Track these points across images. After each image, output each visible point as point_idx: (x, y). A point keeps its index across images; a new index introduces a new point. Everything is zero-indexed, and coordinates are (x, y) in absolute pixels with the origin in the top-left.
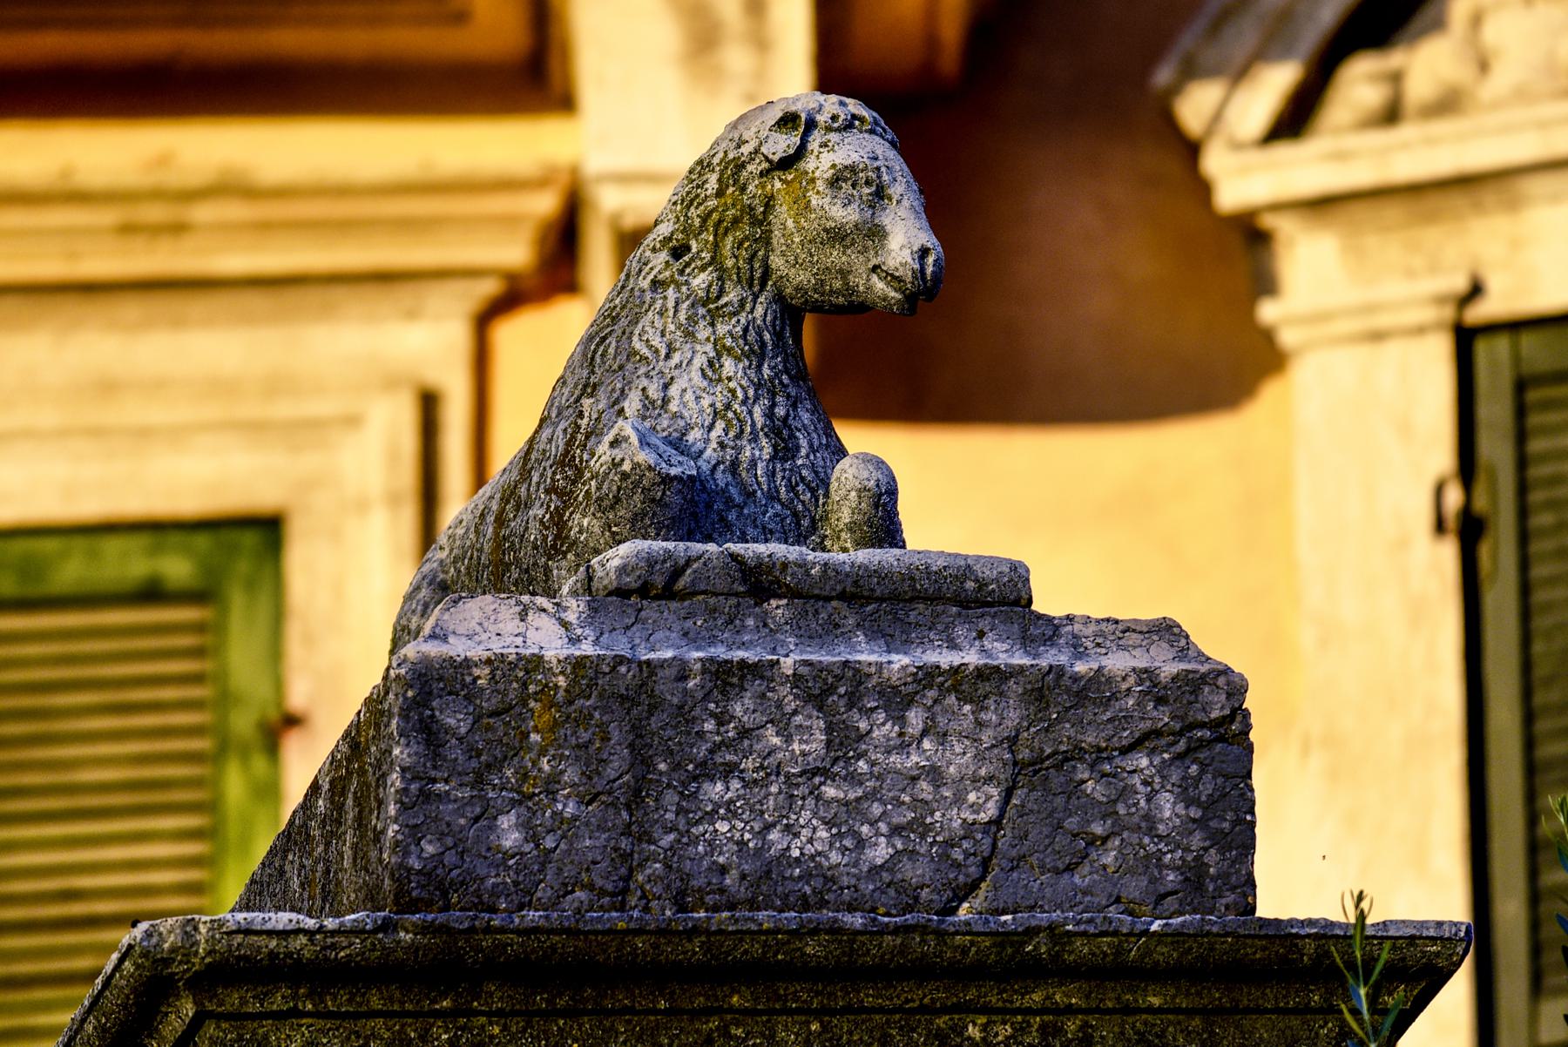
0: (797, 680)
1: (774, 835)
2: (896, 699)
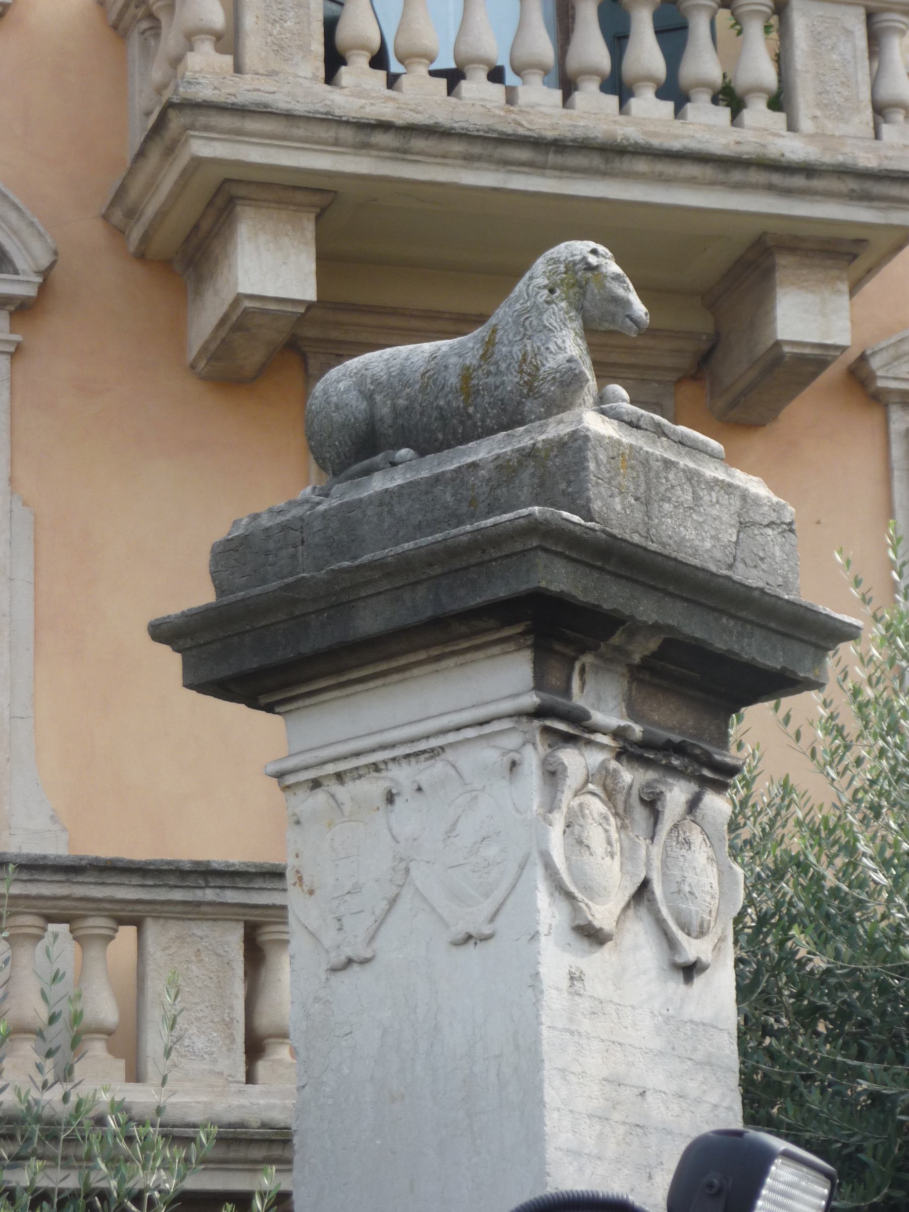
0: (684, 471)
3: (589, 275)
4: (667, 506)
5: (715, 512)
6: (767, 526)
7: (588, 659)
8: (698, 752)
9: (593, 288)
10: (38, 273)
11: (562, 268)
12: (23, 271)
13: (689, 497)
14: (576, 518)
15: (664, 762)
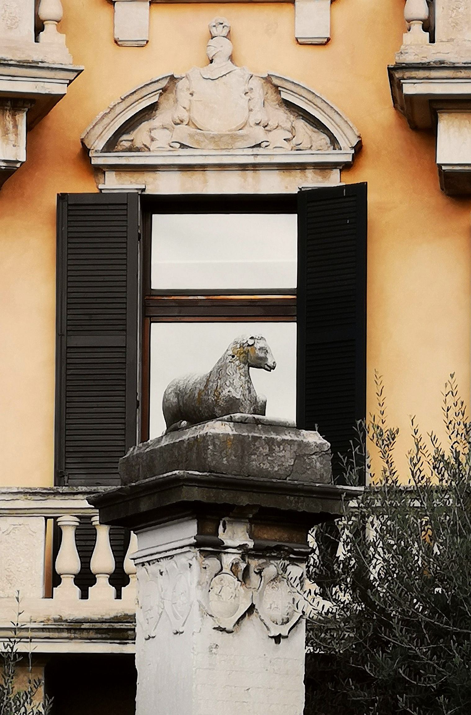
0: (264, 440)
1: (261, 465)
2: (279, 444)
3: (249, 348)
4: (253, 456)
5: (281, 454)
6: (314, 454)
7: (226, 519)
8: (286, 548)
9: (251, 354)
10: (352, 148)
11: (238, 346)
12: (344, 147)
13: (267, 451)
14: (197, 473)
15: (268, 555)
